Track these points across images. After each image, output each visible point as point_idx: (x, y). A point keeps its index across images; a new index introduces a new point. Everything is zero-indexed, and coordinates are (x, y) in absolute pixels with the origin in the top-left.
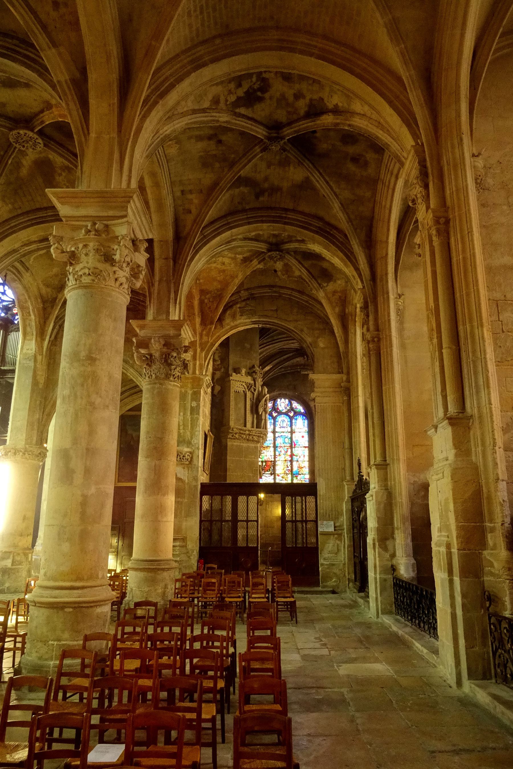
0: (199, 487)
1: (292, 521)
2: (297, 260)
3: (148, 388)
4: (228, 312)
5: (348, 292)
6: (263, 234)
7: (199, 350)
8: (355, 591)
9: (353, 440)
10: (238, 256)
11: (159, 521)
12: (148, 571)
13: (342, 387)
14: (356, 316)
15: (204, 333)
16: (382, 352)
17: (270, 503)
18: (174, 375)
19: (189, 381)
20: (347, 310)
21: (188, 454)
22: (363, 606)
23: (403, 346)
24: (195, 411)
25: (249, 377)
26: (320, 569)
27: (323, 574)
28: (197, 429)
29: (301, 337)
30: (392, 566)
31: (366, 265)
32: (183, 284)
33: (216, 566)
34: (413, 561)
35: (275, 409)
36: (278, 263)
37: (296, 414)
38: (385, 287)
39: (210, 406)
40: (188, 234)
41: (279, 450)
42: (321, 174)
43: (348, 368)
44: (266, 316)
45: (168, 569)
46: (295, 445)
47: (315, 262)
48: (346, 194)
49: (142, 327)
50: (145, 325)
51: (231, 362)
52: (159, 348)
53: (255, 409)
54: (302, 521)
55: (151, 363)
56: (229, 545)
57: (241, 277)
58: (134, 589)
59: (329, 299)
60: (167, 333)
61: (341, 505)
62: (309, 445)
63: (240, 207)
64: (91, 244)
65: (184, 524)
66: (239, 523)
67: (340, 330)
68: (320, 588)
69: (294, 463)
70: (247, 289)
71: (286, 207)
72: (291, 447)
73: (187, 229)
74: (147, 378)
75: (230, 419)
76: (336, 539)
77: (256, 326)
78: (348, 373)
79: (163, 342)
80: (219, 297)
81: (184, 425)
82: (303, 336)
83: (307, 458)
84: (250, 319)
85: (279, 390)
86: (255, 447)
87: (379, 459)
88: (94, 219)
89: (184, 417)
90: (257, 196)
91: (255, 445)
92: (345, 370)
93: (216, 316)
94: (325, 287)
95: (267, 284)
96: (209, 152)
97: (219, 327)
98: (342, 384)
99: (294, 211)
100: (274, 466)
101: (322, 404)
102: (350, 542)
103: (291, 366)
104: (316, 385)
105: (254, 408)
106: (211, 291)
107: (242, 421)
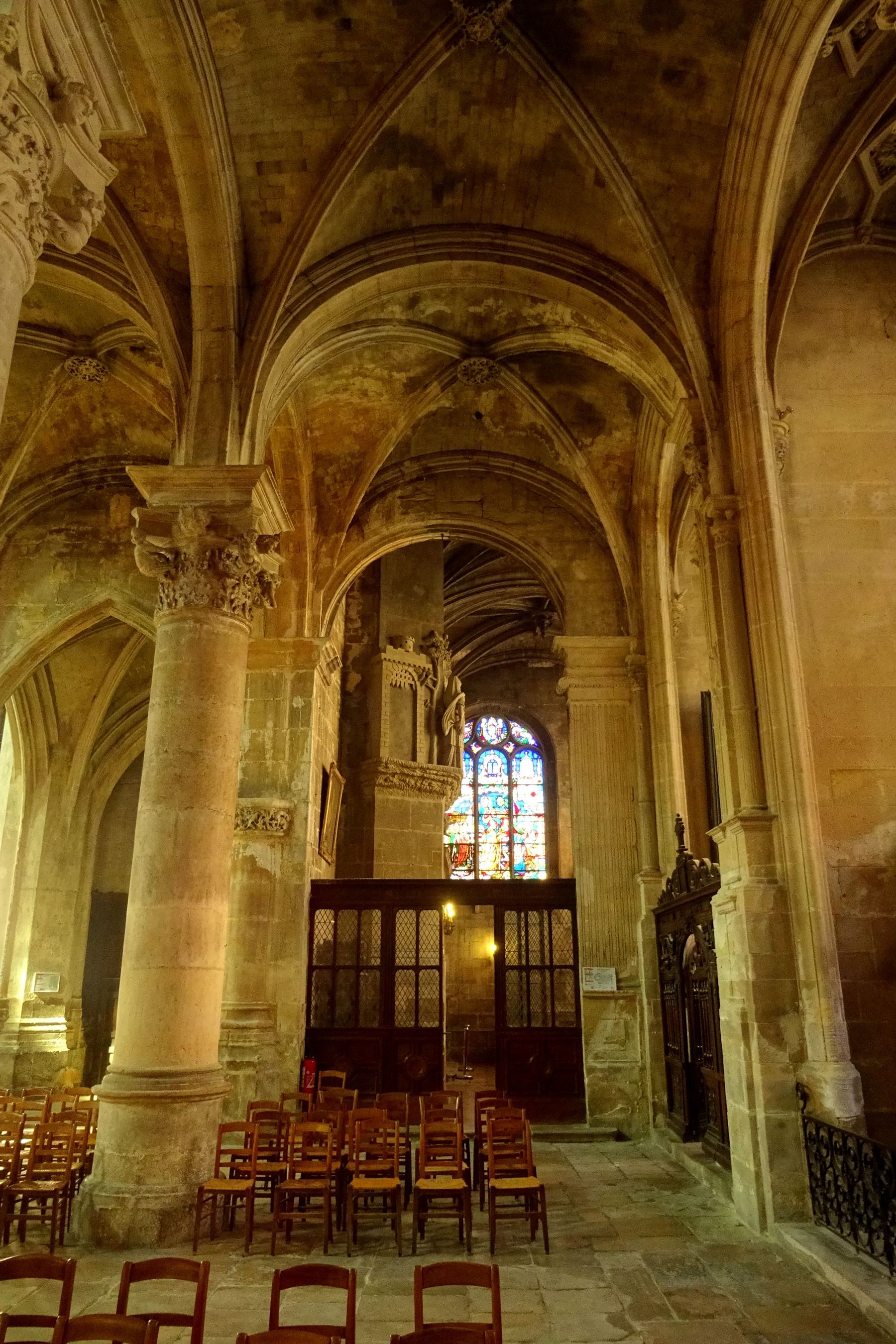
0: (308, 888)
1: (519, 968)
2: (526, 383)
3: (166, 632)
4: (375, 508)
5: (638, 455)
6: (452, 316)
7: (310, 586)
8: (675, 1136)
9: (656, 781)
10: (396, 375)
11: (183, 968)
12: (147, 1105)
13: (626, 665)
14: (656, 509)
15: (324, 549)
16: (744, 541)
17: (468, 931)
18: (232, 601)
19: (288, 652)
20: (635, 499)
21: (282, 813)
22: (705, 1183)
23: (794, 532)
24: (300, 717)
25: (423, 656)
26: (586, 1081)
27: (593, 1093)
28: (305, 758)
29: (535, 558)
30: (799, 1086)
31: (699, 343)
32: (260, 392)
33: (343, 1075)
34: (854, 1073)
35: (476, 738)
36: (484, 394)
37: (520, 747)
38: (746, 390)
39: (337, 714)
40: (274, 271)
41: (485, 821)
42: (590, 117)
43: (641, 623)
44: (458, 515)
45: (203, 1097)
46: (517, 811)
47: (564, 388)
48: (652, 172)
49: (157, 485)
50: (163, 479)
51: (384, 622)
52: (196, 535)
53: (435, 724)
54: (541, 968)
55: (177, 571)
56: (376, 1025)
57: (404, 424)
58: (108, 1152)
59: (596, 475)
60: (219, 498)
61: (633, 931)
62: (546, 810)
63: (398, 222)
65: (271, 974)
66: (397, 974)
67: (621, 542)
68: (587, 1126)
69: (517, 849)
70: (418, 459)
71: (505, 222)
72: (510, 815)
73: (272, 260)
74: (165, 607)
75: (382, 744)
76: (623, 1008)
77: (437, 536)
78: (641, 635)
79: (205, 519)
80: (356, 471)
81: (274, 747)
82: (539, 557)
83: (542, 838)
84: (423, 520)
85: (485, 700)
86: (435, 805)
87: (747, 805)
89: (275, 732)
90: (438, 193)
91: (437, 801)
92: (633, 629)
93: (349, 513)
94: (587, 446)
95: (462, 448)
96: (320, 55)
97: (355, 537)
98: (628, 659)
99: (522, 231)
100: (475, 854)
101: (584, 704)
102: (656, 1014)
103: (506, 652)
104: (570, 660)
105: (433, 722)
106: (339, 458)
107: (407, 749)
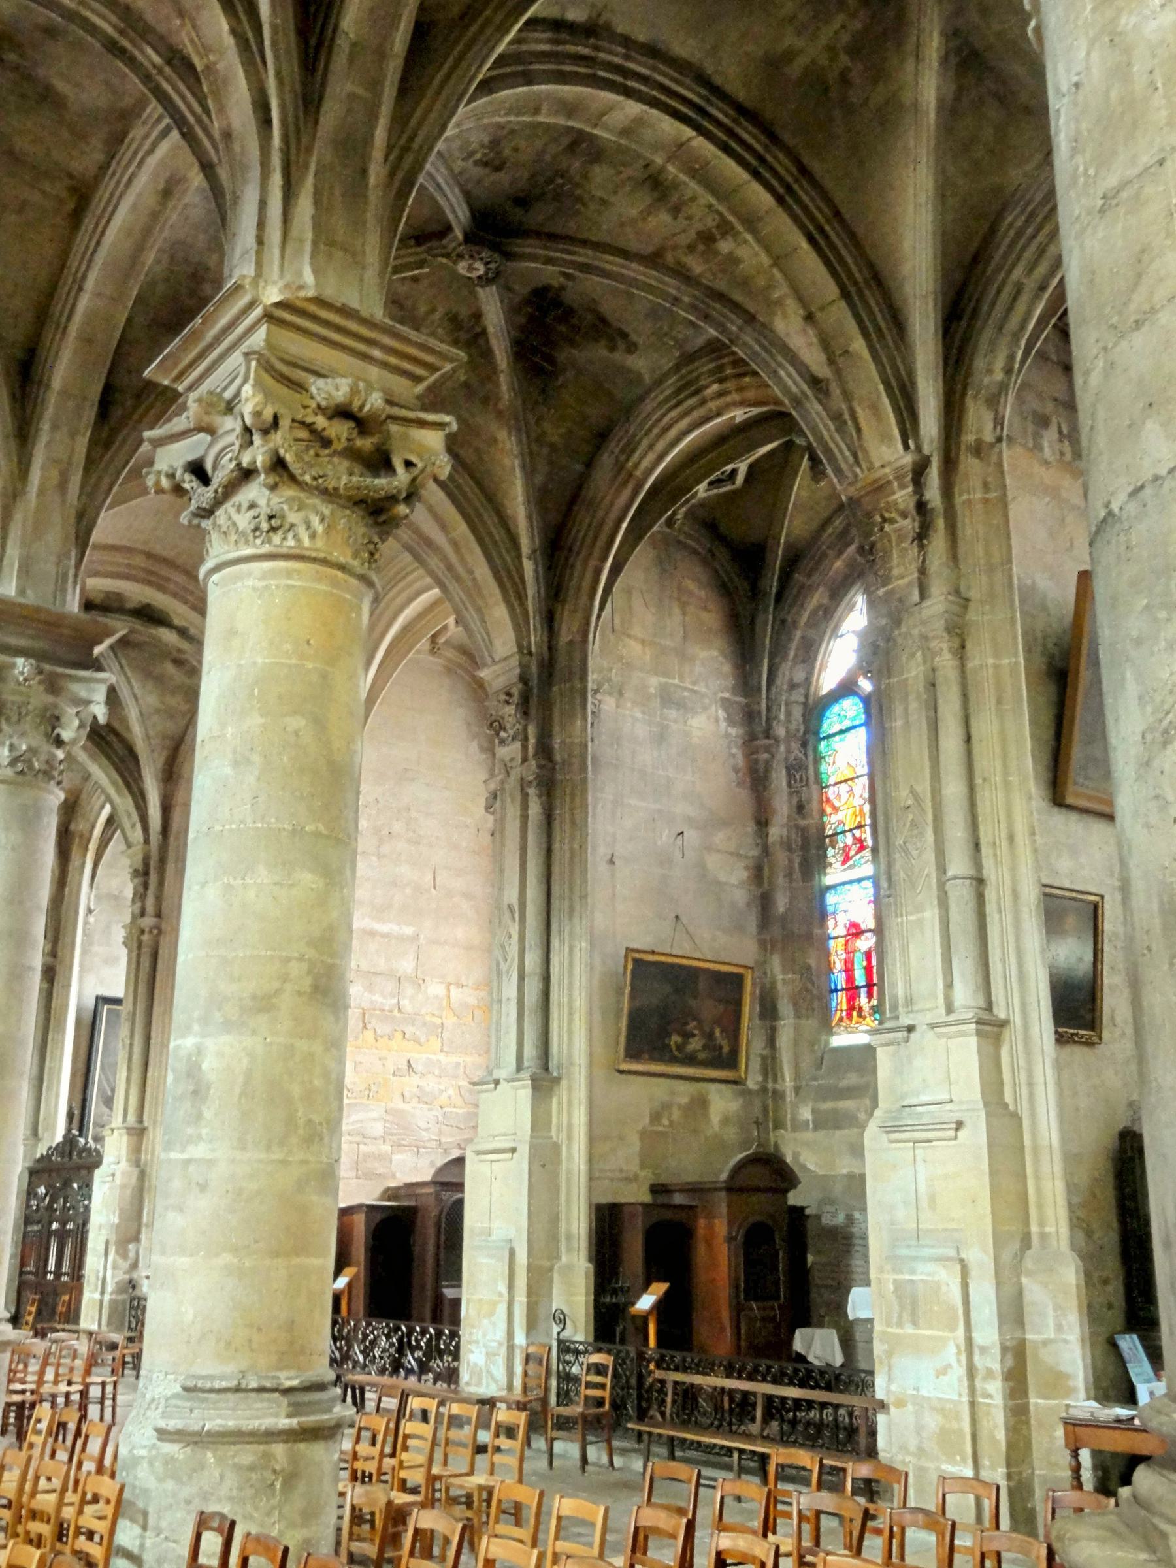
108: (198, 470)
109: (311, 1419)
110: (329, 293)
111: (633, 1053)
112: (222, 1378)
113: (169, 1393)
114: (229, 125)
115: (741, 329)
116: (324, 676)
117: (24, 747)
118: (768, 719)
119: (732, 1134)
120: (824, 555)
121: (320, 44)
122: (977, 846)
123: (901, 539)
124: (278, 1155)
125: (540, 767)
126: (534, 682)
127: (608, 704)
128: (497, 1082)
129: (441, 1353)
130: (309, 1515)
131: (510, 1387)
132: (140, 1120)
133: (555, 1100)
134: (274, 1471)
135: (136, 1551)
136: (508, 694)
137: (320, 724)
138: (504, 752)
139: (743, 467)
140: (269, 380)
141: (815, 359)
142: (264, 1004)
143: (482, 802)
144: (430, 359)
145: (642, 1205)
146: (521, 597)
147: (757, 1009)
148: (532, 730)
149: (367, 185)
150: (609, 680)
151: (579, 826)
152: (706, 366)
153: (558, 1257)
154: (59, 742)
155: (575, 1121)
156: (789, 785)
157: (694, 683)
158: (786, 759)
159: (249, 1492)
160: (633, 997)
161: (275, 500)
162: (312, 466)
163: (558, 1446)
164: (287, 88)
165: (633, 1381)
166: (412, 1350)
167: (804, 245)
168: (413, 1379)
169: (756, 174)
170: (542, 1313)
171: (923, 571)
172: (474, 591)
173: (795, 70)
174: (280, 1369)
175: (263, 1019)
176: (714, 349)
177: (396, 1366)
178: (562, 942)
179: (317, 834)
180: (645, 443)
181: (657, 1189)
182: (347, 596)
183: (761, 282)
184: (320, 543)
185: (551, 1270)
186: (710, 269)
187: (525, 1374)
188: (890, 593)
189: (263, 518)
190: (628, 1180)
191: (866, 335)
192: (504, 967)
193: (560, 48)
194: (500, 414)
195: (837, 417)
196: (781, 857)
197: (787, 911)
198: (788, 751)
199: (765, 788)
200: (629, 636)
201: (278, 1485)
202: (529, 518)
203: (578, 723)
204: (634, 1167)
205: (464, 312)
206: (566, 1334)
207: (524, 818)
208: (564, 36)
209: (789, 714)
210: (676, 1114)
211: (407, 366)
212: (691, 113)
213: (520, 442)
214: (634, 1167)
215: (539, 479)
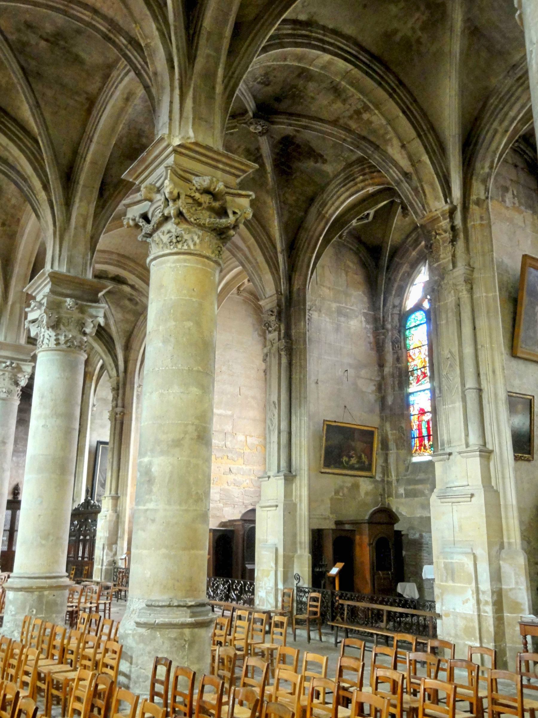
64: (7, 373)
88: (12, 359)
108: (145, 217)
109: (200, 619)
110: (200, 140)
111: (327, 464)
112: (163, 601)
113: (140, 607)
114: (156, 70)
115: (373, 152)
116: (201, 304)
117: (70, 336)
118: (384, 321)
119: (369, 499)
120: (407, 250)
121: (194, 33)
122: (479, 375)
123: (444, 242)
124: (184, 507)
125: (286, 342)
126: (283, 307)
127: (315, 315)
128: (269, 477)
129: (246, 592)
130: (200, 659)
131: (276, 606)
132: (117, 493)
133: (294, 485)
134: (185, 640)
135: (128, 673)
136: (272, 311)
137: (198, 324)
138: (270, 336)
139: (372, 212)
140: (176, 179)
141: (404, 163)
142: (177, 443)
143: (261, 358)
144: (243, 167)
145: (332, 530)
146: (277, 270)
147: (380, 446)
148: (282, 327)
149: (214, 93)
150: (315, 305)
151: (303, 367)
152: (356, 169)
153: (296, 551)
154: (85, 334)
155: (303, 494)
156: (393, 349)
157: (352, 306)
158: (392, 338)
159: (174, 649)
160: (327, 440)
161: (179, 229)
162: (193, 214)
163: (298, 632)
164: (181, 53)
165: (330, 604)
166: (234, 590)
167: (401, 114)
168: (234, 603)
169: (380, 84)
170: (290, 575)
171: (454, 256)
172: (257, 267)
173: (398, 38)
174: (186, 598)
175: (177, 450)
176: (361, 161)
177: (227, 597)
178: (296, 416)
179: (198, 371)
180: (330, 202)
181: (338, 523)
182: (209, 270)
183: (382, 132)
184: (197, 247)
185: (293, 557)
186: (359, 127)
187: (283, 601)
188: (439, 265)
189: (174, 237)
190: (325, 519)
191: (428, 153)
192: (271, 428)
193: (295, 32)
194: (267, 192)
195: (415, 190)
196: (390, 381)
197: (393, 403)
198: (393, 335)
199: (383, 351)
200: (324, 286)
201: (187, 646)
202: (281, 236)
203: (302, 323)
204: (327, 513)
205: (252, 148)
206: (300, 584)
207: (280, 364)
208: (298, 27)
209: (392, 319)
210: (346, 490)
211: (233, 171)
212: (353, 59)
213: (276, 203)
214: (327, 513)
215: (285, 219)
